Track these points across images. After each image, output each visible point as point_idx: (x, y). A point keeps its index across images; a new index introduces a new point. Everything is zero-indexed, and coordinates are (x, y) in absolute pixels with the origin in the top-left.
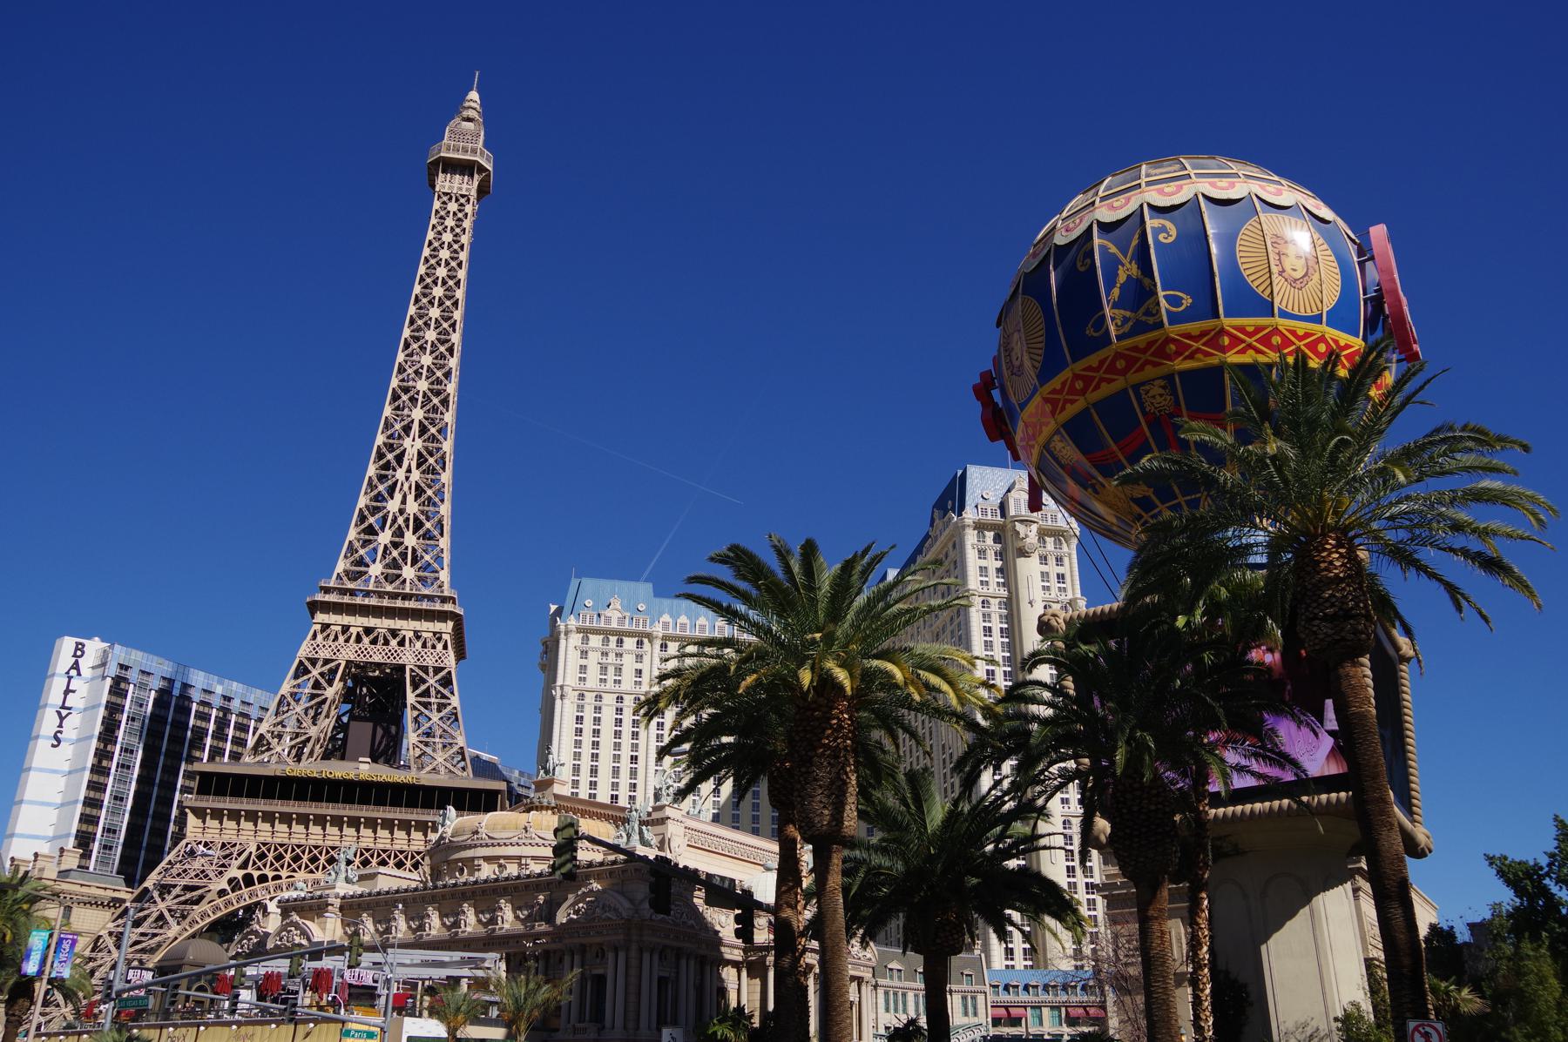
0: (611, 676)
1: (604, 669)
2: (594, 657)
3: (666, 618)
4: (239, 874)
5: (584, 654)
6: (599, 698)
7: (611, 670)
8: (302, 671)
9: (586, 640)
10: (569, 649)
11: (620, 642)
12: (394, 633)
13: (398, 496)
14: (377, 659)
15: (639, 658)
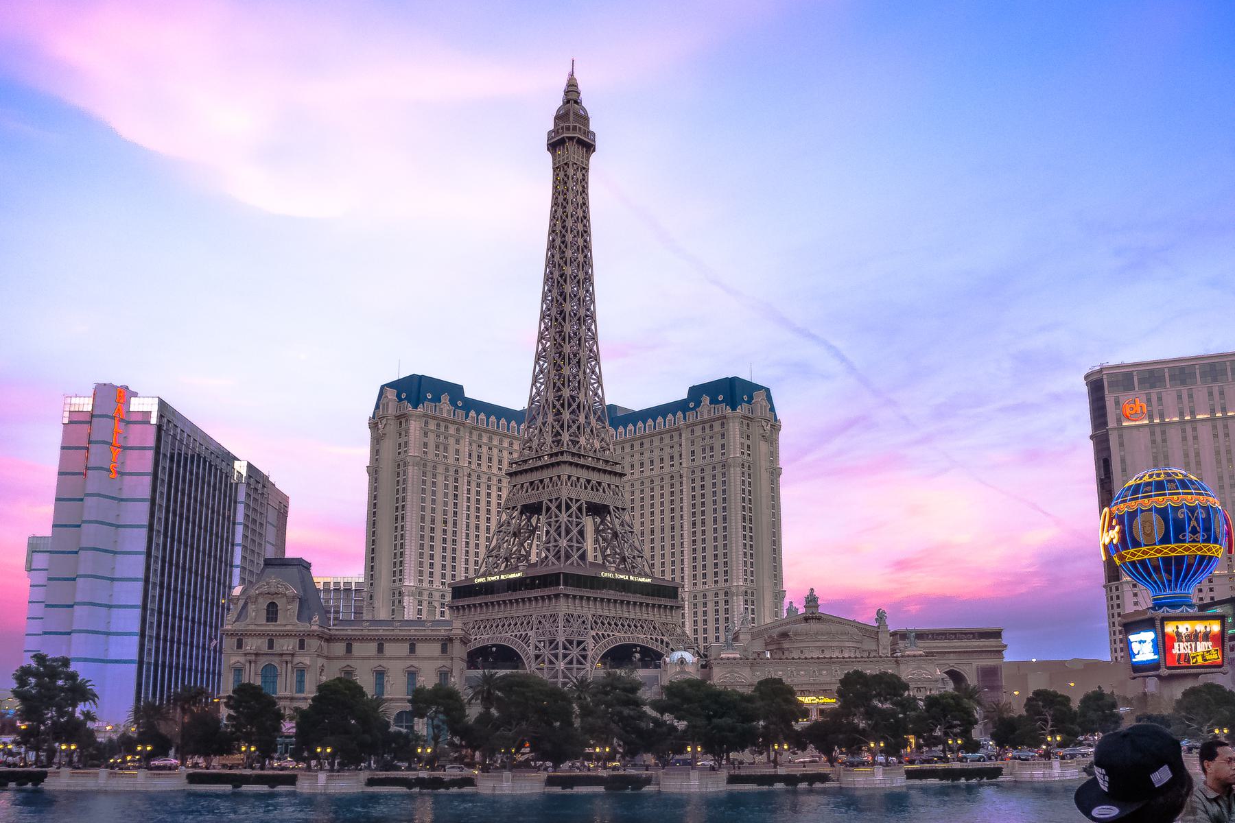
0: (441, 452)
1: (437, 447)
2: (432, 436)
3: (472, 413)
4: (593, 633)
5: (426, 434)
6: (435, 467)
7: (442, 448)
8: (568, 507)
9: (426, 423)
10: (415, 427)
11: (446, 427)
12: (599, 484)
13: (583, 390)
14: (597, 500)
15: (457, 442)
